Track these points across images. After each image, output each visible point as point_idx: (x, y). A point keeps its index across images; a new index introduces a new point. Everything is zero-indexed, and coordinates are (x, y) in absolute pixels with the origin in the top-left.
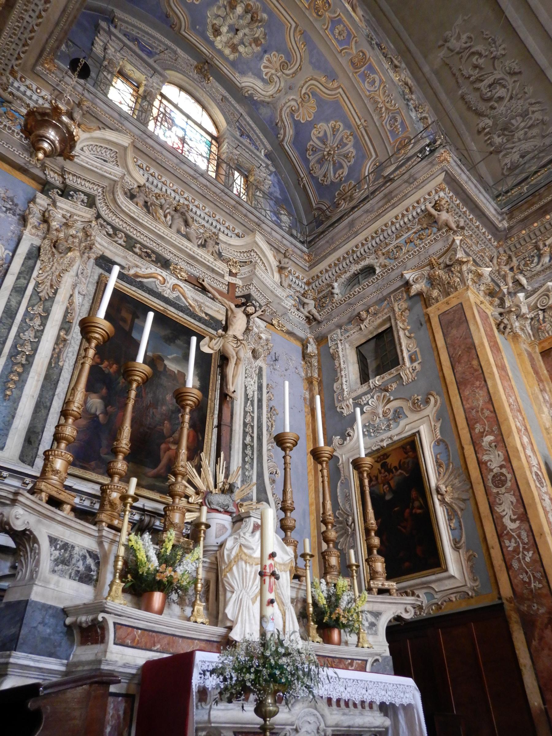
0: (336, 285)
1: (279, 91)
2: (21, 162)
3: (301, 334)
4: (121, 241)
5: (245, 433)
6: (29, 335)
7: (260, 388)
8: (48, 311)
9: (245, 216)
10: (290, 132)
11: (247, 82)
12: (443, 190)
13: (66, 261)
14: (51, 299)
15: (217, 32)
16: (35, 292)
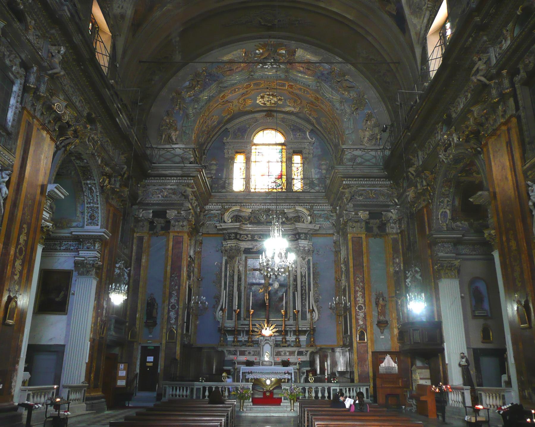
0: (338, 208)
1: (300, 109)
2: (216, 232)
3: (331, 232)
4: (250, 239)
5: (302, 290)
6: (231, 288)
7: (309, 269)
8: (233, 279)
9: (291, 198)
10: (314, 121)
11: (287, 109)
12: (344, 180)
13: (234, 261)
14: (233, 275)
15: (265, 104)
16: (230, 274)
